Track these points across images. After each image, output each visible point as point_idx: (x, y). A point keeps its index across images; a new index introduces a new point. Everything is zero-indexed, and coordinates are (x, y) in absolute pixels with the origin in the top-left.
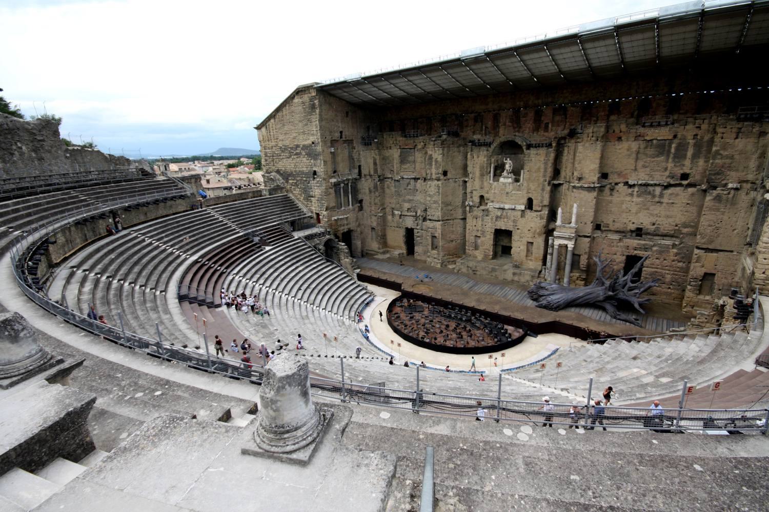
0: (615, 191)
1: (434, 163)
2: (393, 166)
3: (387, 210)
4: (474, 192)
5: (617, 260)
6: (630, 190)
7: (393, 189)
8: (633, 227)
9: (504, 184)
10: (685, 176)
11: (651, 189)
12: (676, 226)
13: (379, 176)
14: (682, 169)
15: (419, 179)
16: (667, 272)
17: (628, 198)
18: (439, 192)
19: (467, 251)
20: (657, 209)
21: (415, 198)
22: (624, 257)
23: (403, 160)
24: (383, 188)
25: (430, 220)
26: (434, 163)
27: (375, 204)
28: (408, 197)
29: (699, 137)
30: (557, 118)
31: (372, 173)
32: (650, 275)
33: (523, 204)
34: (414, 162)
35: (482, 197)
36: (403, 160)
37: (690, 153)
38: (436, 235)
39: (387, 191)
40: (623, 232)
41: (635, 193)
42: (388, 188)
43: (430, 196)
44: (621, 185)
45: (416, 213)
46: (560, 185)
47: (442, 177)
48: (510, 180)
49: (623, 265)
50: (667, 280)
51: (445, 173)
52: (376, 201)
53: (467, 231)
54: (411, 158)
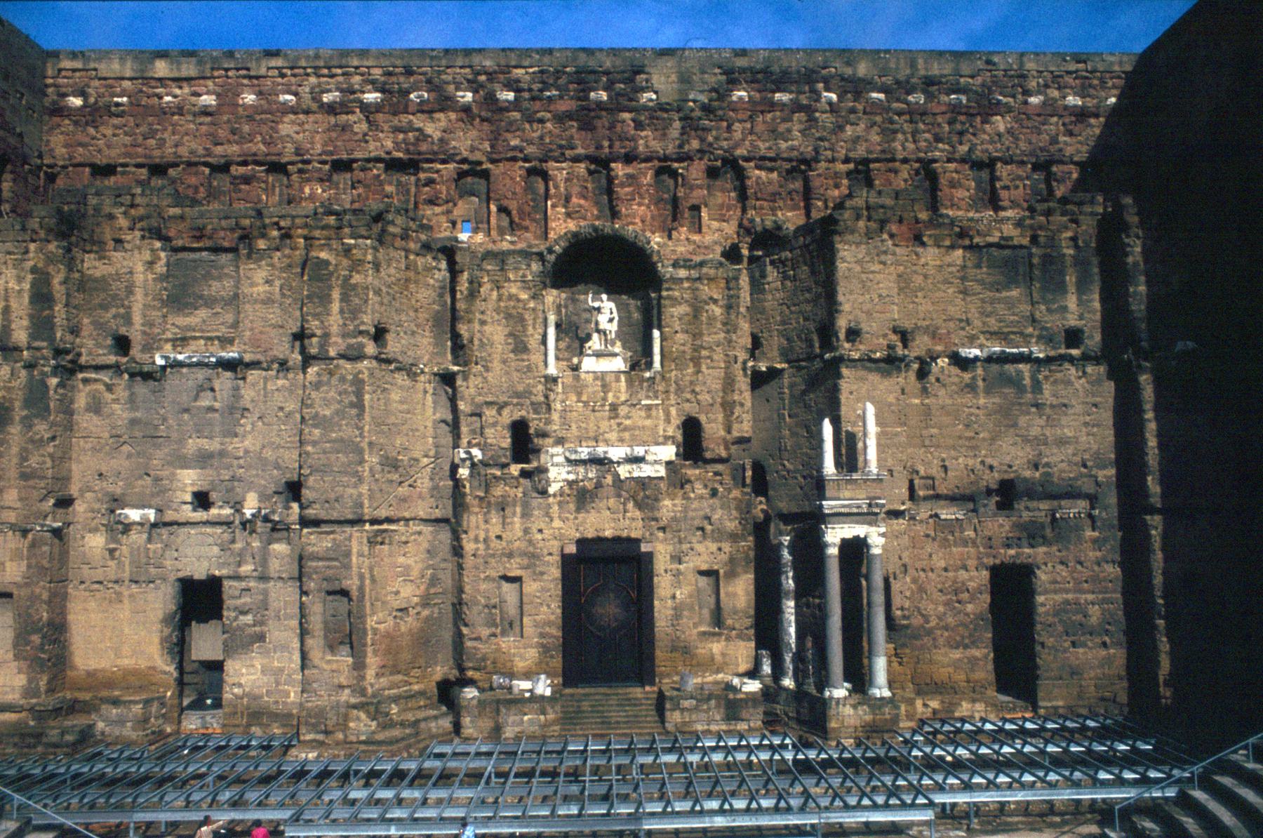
0: (932, 379)
1: (336, 295)
2: (128, 319)
3: (80, 507)
4: (490, 413)
5: (972, 585)
6: (967, 376)
7: (121, 413)
8: (992, 479)
9: (601, 377)
10: (1073, 337)
11: (1010, 368)
12: (1085, 466)
13: (58, 352)
14: (1064, 319)
15: (255, 365)
16: (1090, 597)
17: (968, 399)
18: (360, 406)
19: (469, 644)
20: (1034, 425)
21: (237, 446)
22: (985, 574)
23: (179, 296)
24: (68, 410)
25: (316, 523)
26: (336, 295)
27: (24, 476)
28: (193, 444)
29: (1080, 243)
30: (720, 198)
31: (20, 335)
32: (1054, 616)
33: (667, 439)
34: (234, 300)
35: (520, 430)
36: (179, 296)
37: (1070, 279)
38: (346, 584)
39: (86, 421)
40: (971, 498)
41: (980, 383)
42: (96, 407)
43: (319, 421)
44: (943, 362)
45: (238, 506)
46: (773, 374)
47: (371, 349)
48: (618, 364)
49: (986, 598)
50: (1094, 620)
51: (379, 335)
52: (34, 461)
53: (469, 562)
54: (219, 288)
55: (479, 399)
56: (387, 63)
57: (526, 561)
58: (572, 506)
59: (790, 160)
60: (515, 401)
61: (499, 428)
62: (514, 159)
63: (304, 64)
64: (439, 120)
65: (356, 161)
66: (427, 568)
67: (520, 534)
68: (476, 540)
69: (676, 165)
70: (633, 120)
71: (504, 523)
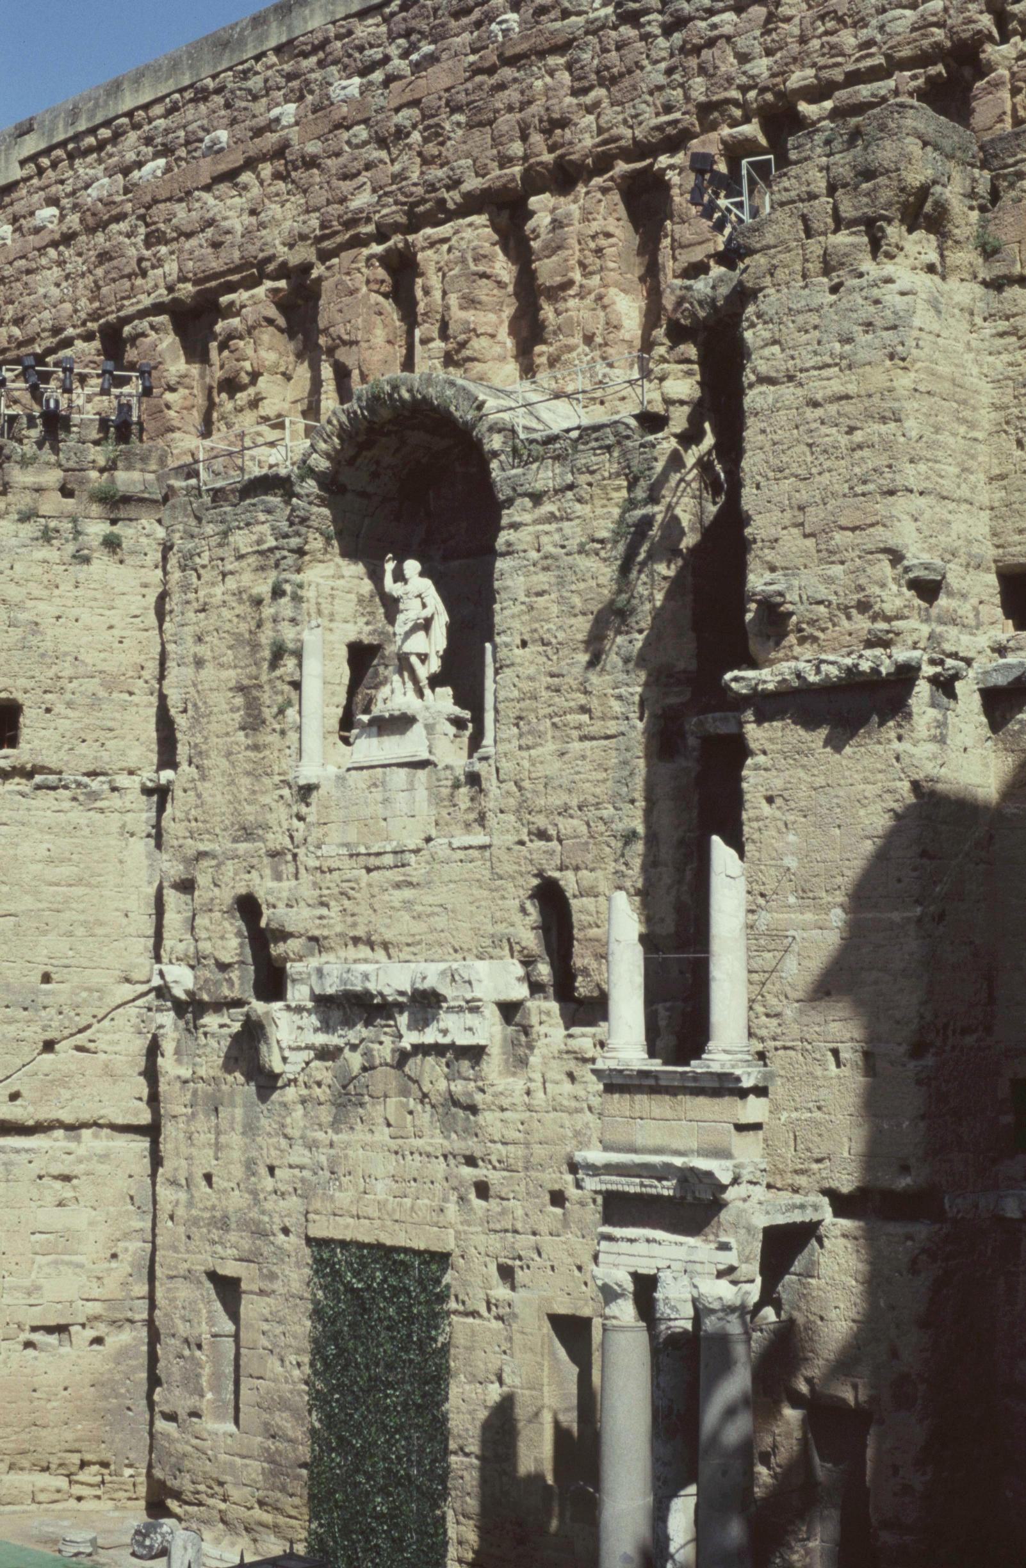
55: (193, 846)
56: (171, 86)
57: (246, 1244)
58: (325, 1114)
59: (922, 60)
60: (243, 847)
61: (217, 915)
62: (358, 242)
63: (60, 137)
64: (245, 188)
65: (128, 320)
66: (126, 1236)
67: (238, 1172)
68: (174, 1183)
69: (663, 160)
70: (569, 67)
71: (217, 1143)
